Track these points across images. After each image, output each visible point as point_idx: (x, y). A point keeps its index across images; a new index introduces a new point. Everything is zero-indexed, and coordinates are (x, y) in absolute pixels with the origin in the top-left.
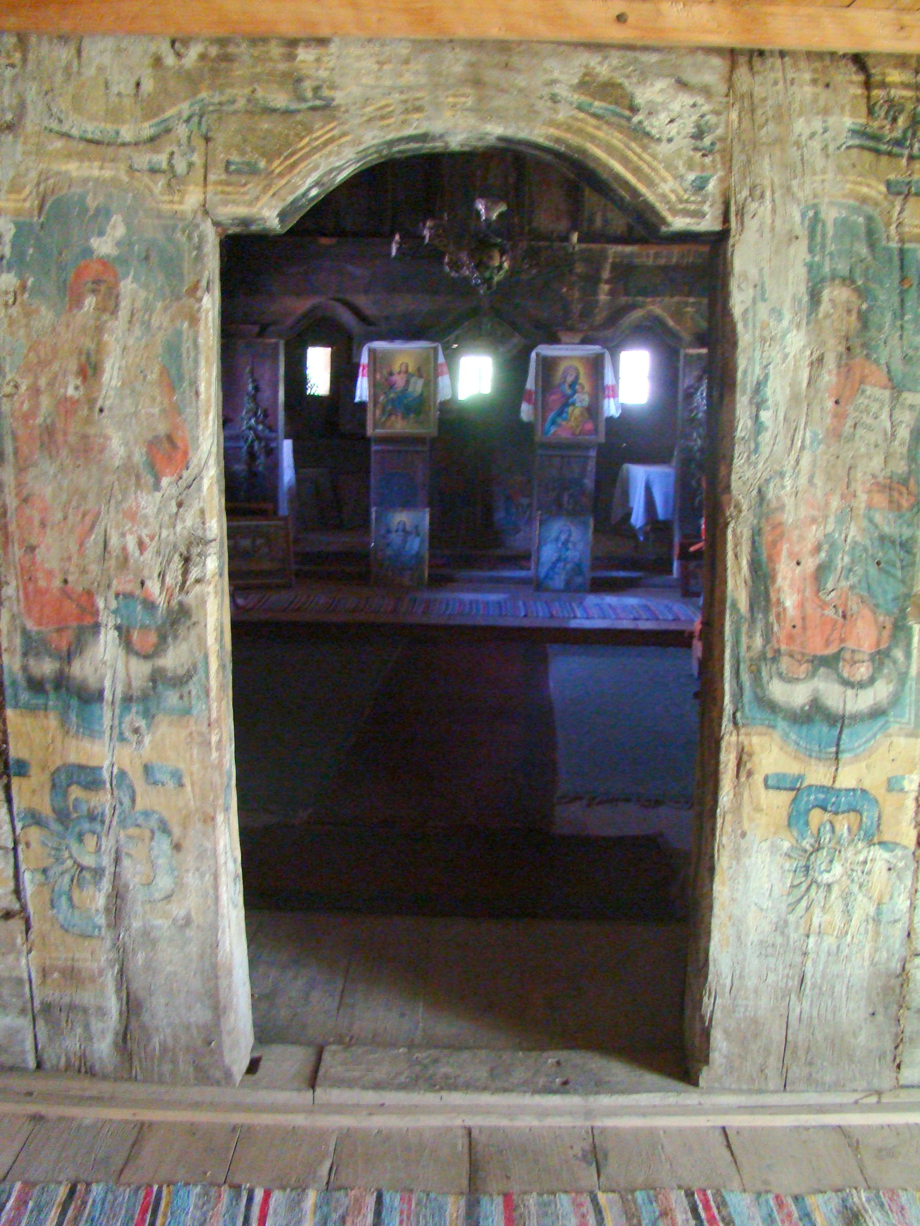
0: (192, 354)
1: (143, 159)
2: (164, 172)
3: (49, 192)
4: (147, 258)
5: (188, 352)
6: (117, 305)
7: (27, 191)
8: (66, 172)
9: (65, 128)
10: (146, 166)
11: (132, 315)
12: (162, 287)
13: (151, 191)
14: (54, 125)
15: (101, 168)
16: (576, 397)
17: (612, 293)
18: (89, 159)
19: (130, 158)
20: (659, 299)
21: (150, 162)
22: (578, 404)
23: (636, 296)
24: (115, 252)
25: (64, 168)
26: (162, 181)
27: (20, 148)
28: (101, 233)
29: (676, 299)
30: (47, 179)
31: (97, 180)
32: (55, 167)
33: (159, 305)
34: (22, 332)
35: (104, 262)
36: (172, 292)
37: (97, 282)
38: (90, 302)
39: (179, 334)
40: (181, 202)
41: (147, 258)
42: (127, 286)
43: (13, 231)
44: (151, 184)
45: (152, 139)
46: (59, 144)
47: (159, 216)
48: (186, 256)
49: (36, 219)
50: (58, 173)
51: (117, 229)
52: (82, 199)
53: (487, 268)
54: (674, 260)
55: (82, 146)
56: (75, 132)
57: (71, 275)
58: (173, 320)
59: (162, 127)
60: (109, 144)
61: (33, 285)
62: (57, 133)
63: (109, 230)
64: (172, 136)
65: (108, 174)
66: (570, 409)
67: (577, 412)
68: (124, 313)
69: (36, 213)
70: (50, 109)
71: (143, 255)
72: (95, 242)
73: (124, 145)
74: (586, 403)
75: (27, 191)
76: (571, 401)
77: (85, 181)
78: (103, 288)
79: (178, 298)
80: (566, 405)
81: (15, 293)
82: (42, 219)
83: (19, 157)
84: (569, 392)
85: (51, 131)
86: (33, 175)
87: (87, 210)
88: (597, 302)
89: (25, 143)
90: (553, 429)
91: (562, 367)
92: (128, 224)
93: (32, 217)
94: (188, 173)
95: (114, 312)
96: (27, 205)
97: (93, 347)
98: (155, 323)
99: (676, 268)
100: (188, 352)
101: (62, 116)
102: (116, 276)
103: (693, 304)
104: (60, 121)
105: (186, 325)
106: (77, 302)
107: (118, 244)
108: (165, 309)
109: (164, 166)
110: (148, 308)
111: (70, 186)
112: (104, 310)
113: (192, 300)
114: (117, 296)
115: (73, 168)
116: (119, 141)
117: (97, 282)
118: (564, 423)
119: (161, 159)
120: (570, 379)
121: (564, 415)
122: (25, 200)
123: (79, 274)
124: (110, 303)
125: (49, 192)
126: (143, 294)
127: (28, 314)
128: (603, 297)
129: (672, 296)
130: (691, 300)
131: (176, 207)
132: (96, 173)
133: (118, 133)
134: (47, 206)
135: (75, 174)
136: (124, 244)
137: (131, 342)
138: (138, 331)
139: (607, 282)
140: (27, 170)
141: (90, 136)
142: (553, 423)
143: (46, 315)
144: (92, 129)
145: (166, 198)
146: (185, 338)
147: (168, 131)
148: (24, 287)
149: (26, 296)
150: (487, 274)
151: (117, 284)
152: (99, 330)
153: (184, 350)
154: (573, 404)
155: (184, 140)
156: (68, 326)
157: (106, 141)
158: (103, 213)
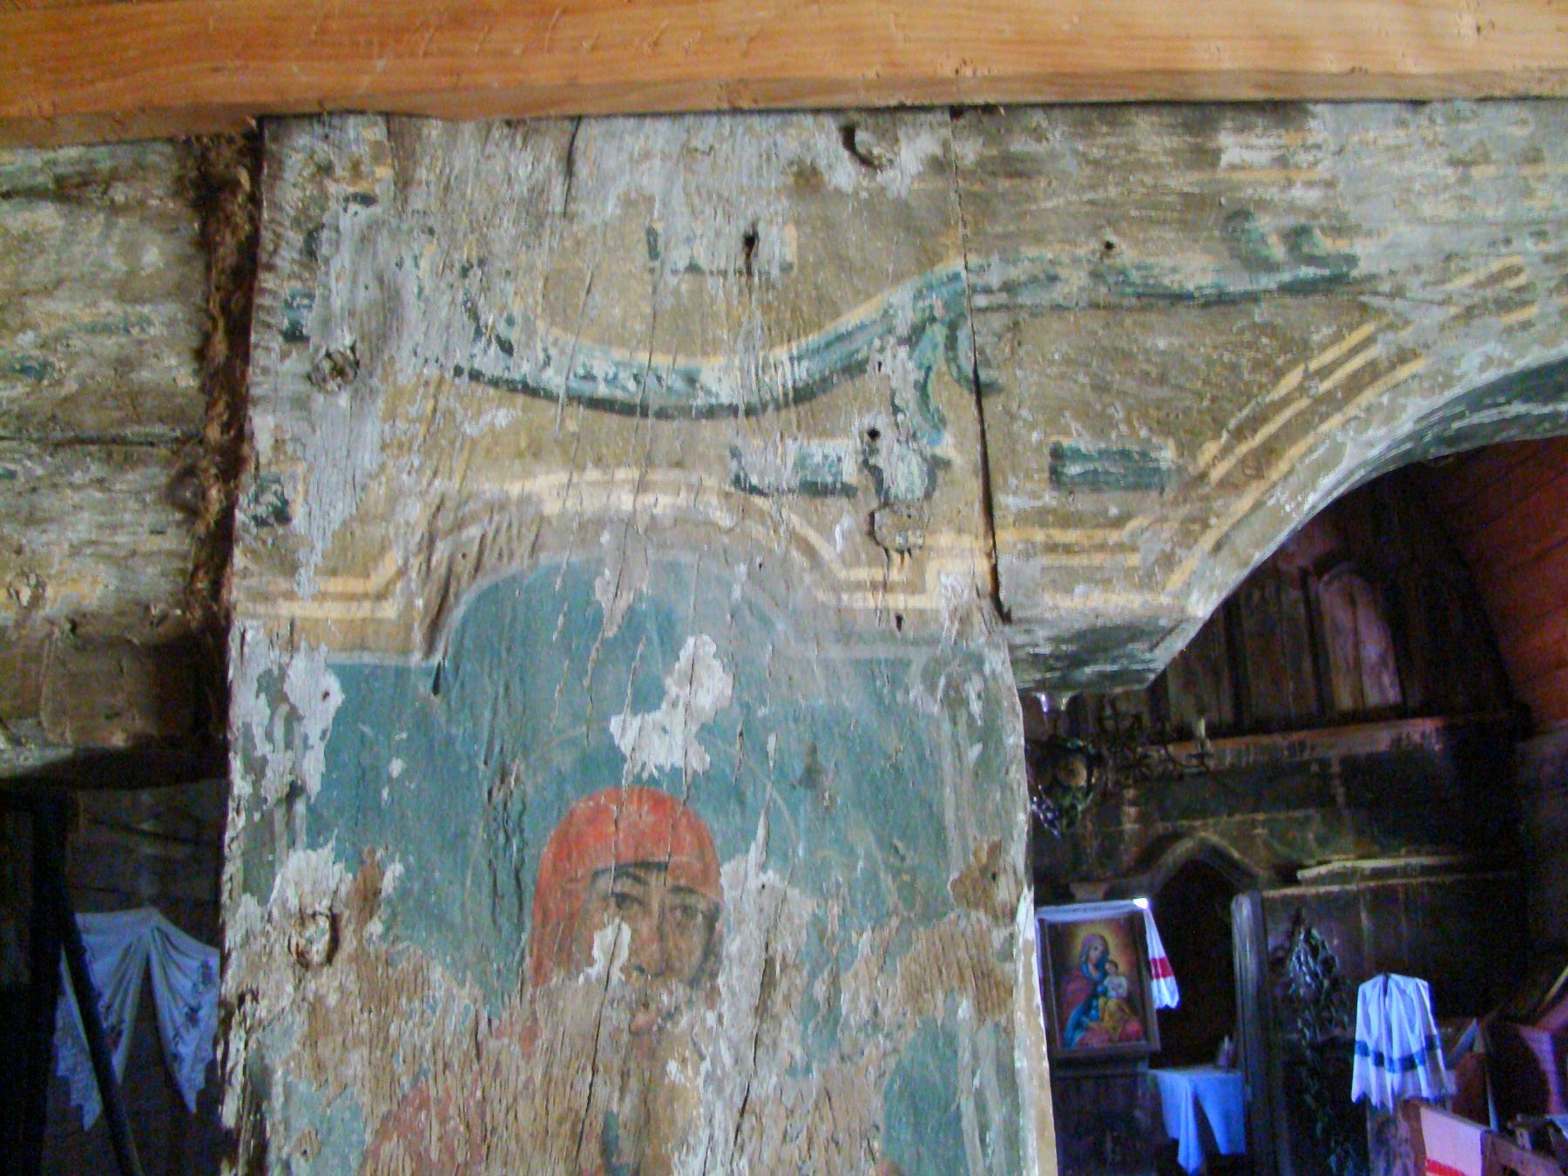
0: (996, 1116)
1: (777, 456)
2: (848, 491)
3: (464, 567)
4: (811, 777)
5: (981, 1108)
6: (711, 950)
7: (391, 563)
8: (525, 500)
9: (524, 369)
10: (789, 478)
11: (768, 982)
12: (872, 876)
13: (810, 552)
14: (490, 361)
15: (641, 487)
16: (1106, 982)
17: (1142, 818)
18: (599, 462)
19: (735, 453)
20: (1211, 821)
21: (801, 463)
22: (1112, 993)
23: (1178, 818)
24: (699, 761)
25: (515, 489)
26: (846, 521)
27: (372, 430)
28: (646, 698)
29: (1238, 817)
30: (460, 525)
31: (629, 523)
32: (489, 487)
33: (864, 943)
34: (357, 1063)
35: (659, 795)
36: (908, 891)
37: (639, 868)
38: (611, 942)
39: (943, 1041)
40: (915, 586)
41: (811, 777)
42: (745, 879)
43: (337, 698)
44: (813, 537)
45: (802, 395)
46: (502, 416)
47: (846, 634)
48: (947, 761)
49: (416, 657)
50: (499, 506)
51: (705, 682)
52: (580, 583)
53: (1067, 789)
54: (1228, 760)
55: (576, 420)
56: (553, 379)
57: (544, 850)
58: (916, 993)
59: (836, 355)
60: (662, 414)
61: (404, 892)
62: (495, 383)
63: (672, 687)
64: (871, 380)
65: (663, 503)
66: (1101, 1001)
67: (1112, 1004)
68: (737, 979)
69: (418, 636)
70: (474, 314)
71: (798, 768)
72: (625, 730)
73: (711, 413)
74: (1123, 991)
75: (391, 563)
76: (1100, 989)
77: (589, 527)
78: (657, 888)
79: (931, 913)
80: (1095, 995)
81: (334, 920)
82: (437, 659)
83: (367, 458)
84: (1095, 974)
85: (475, 376)
86: (415, 512)
87: (597, 623)
88: (1121, 833)
89: (391, 415)
90: (1078, 1037)
91: (1081, 935)
92: (736, 665)
93: (406, 651)
94: (928, 495)
95: (703, 977)
96: (390, 610)
97: (626, 1110)
98: (853, 1006)
99: (1234, 771)
100: (981, 1108)
101: (514, 335)
102: (703, 842)
103: (1264, 824)
104: (507, 348)
105: (965, 1008)
106: (564, 946)
107: (708, 733)
108: (885, 953)
109: (850, 472)
110: (827, 952)
111: (534, 549)
112: (665, 970)
113: (981, 917)
114: (712, 918)
115: (545, 487)
116: (700, 401)
117: (639, 868)
118: (1093, 1025)
119: (839, 453)
120: (1095, 955)
121: (1093, 1012)
122: (381, 596)
123: (568, 845)
124: (685, 943)
125: (464, 567)
126: (802, 905)
127: (379, 997)
128: (1129, 826)
129: (1230, 815)
130: (1261, 817)
131: (899, 601)
132: (625, 501)
133: (691, 380)
134: (457, 615)
135: (551, 508)
136: (738, 731)
137: (767, 1084)
138: (790, 1042)
139: (1133, 803)
140: (395, 498)
141: (602, 390)
142: (1079, 1025)
143: (450, 996)
144: (607, 368)
145: (862, 574)
146: (965, 1057)
147: (854, 368)
148: (368, 898)
149: (376, 927)
150: (1067, 801)
151: (709, 874)
152: (647, 1044)
153: (967, 1107)
154: (1105, 993)
155: (907, 397)
156: (530, 1036)
157: (654, 406)
158: (655, 631)
